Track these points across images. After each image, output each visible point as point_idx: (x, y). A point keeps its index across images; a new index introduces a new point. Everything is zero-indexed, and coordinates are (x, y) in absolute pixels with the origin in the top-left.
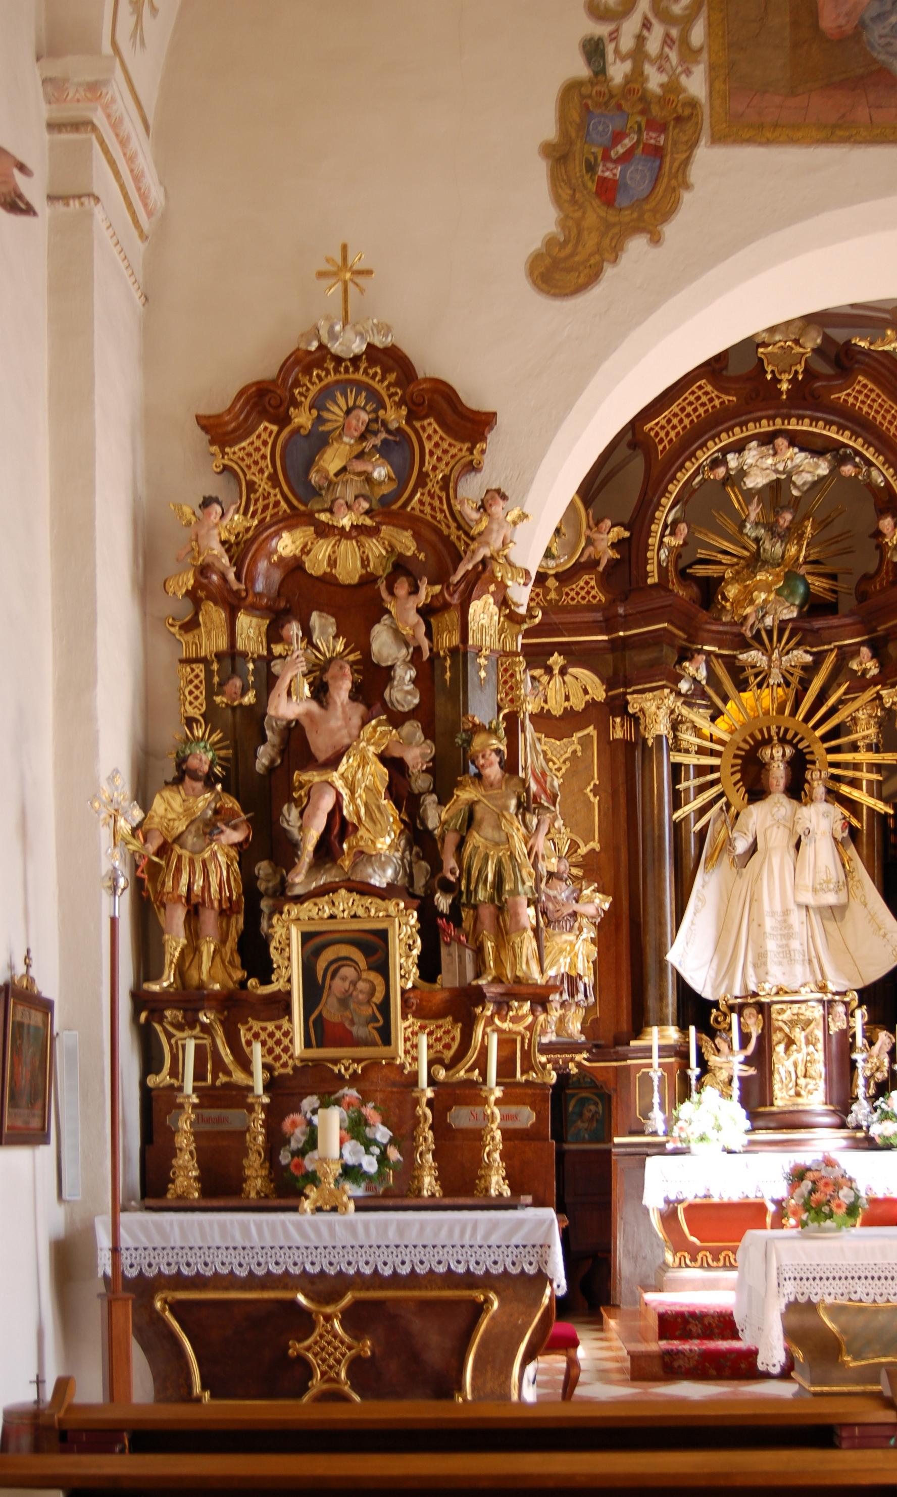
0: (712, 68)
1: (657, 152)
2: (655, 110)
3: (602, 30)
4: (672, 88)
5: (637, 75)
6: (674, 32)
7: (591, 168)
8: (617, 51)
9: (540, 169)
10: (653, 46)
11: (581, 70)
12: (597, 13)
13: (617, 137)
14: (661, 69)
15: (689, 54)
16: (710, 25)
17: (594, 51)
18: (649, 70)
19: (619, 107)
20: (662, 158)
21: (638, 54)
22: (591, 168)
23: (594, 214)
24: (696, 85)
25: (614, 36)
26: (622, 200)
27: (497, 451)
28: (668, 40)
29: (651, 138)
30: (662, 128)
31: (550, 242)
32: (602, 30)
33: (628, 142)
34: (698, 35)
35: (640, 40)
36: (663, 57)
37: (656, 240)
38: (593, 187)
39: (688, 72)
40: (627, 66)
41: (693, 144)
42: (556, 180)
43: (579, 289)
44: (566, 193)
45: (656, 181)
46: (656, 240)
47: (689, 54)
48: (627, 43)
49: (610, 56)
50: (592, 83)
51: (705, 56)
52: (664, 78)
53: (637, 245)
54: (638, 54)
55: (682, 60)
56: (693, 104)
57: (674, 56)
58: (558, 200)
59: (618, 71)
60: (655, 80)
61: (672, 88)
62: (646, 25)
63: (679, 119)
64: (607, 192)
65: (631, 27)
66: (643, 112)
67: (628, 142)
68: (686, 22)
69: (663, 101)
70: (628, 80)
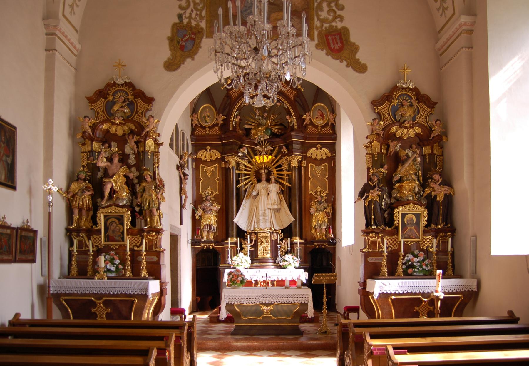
0: (207, 21)
1: (194, 39)
2: (194, 30)
3: (182, 12)
4: (197, 25)
5: (190, 22)
6: (198, 13)
7: (178, 42)
8: (185, 17)
9: (167, 42)
10: (193, 16)
11: (177, 21)
12: (181, 7)
13: (185, 36)
14: (195, 21)
15: (201, 18)
16: (206, 11)
17: (180, 16)
18: (192, 21)
19: (185, 29)
20: (195, 41)
21: (190, 17)
22: (178, 42)
23: (179, 53)
24: (203, 25)
25: (185, 13)
26: (185, 50)
27: (155, 106)
28: (197, 14)
29: (192, 36)
30: (195, 34)
31: (169, 59)
32: (182, 12)
33: (187, 37)
34: (204, 13)
35: (191, 14)
36: (195, 18)
37: (193, 59)
38: (179, 47)
39: (201, 22)
40: (188, 20)
41: (202, 38)
42: (170, 45)
43: (175, 70)
44: (173, 48)
45: (193, 46)
46: (193, 59)
47: (201, 18)
48: (187, 15)
49: (184, 18)
50: (179, 23)
51: (205, 18)
52: (196, 23)
53: (189, 60)
54: (190, 17)
55: (200, 19)
56: (202, 29)
57: (198, 18)
58: (171, 50)
59: (185, 21)
60: (194, 23)
61: (197, 25)
62: (192, 11)
63: (199, 32)
64: (182, 48)
65: (188, 11)
66: (191, 30)
67: (187, 37)
68: (201, 11)
69: (195, 28)
70: (187, 23)
